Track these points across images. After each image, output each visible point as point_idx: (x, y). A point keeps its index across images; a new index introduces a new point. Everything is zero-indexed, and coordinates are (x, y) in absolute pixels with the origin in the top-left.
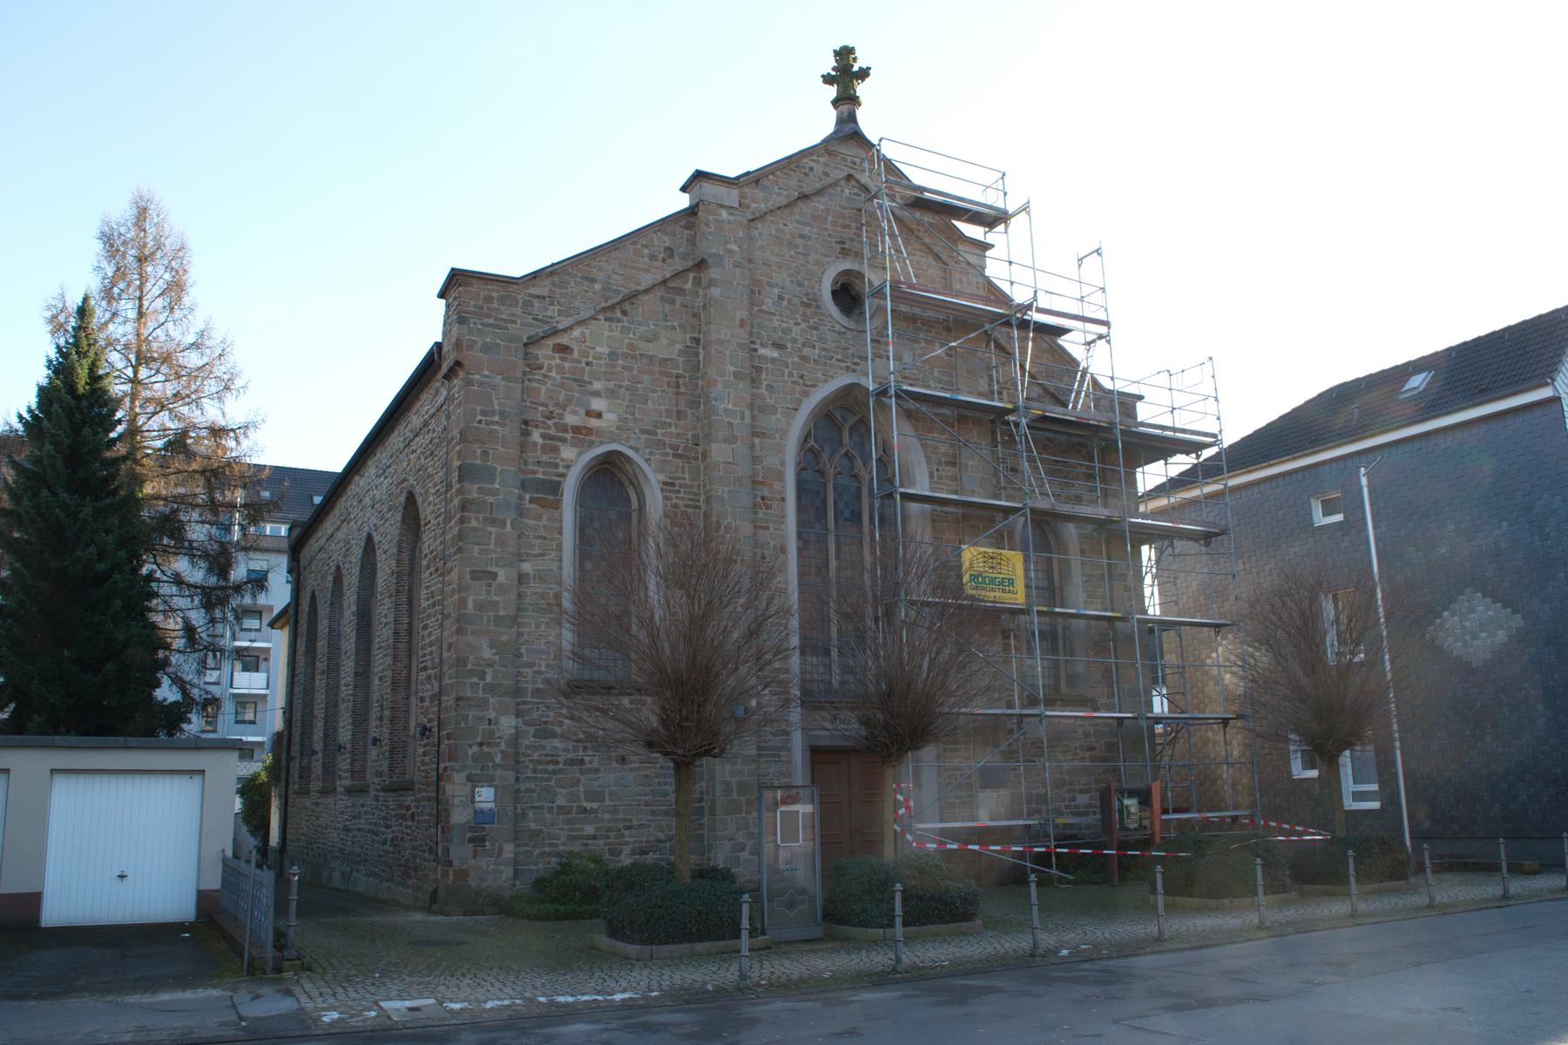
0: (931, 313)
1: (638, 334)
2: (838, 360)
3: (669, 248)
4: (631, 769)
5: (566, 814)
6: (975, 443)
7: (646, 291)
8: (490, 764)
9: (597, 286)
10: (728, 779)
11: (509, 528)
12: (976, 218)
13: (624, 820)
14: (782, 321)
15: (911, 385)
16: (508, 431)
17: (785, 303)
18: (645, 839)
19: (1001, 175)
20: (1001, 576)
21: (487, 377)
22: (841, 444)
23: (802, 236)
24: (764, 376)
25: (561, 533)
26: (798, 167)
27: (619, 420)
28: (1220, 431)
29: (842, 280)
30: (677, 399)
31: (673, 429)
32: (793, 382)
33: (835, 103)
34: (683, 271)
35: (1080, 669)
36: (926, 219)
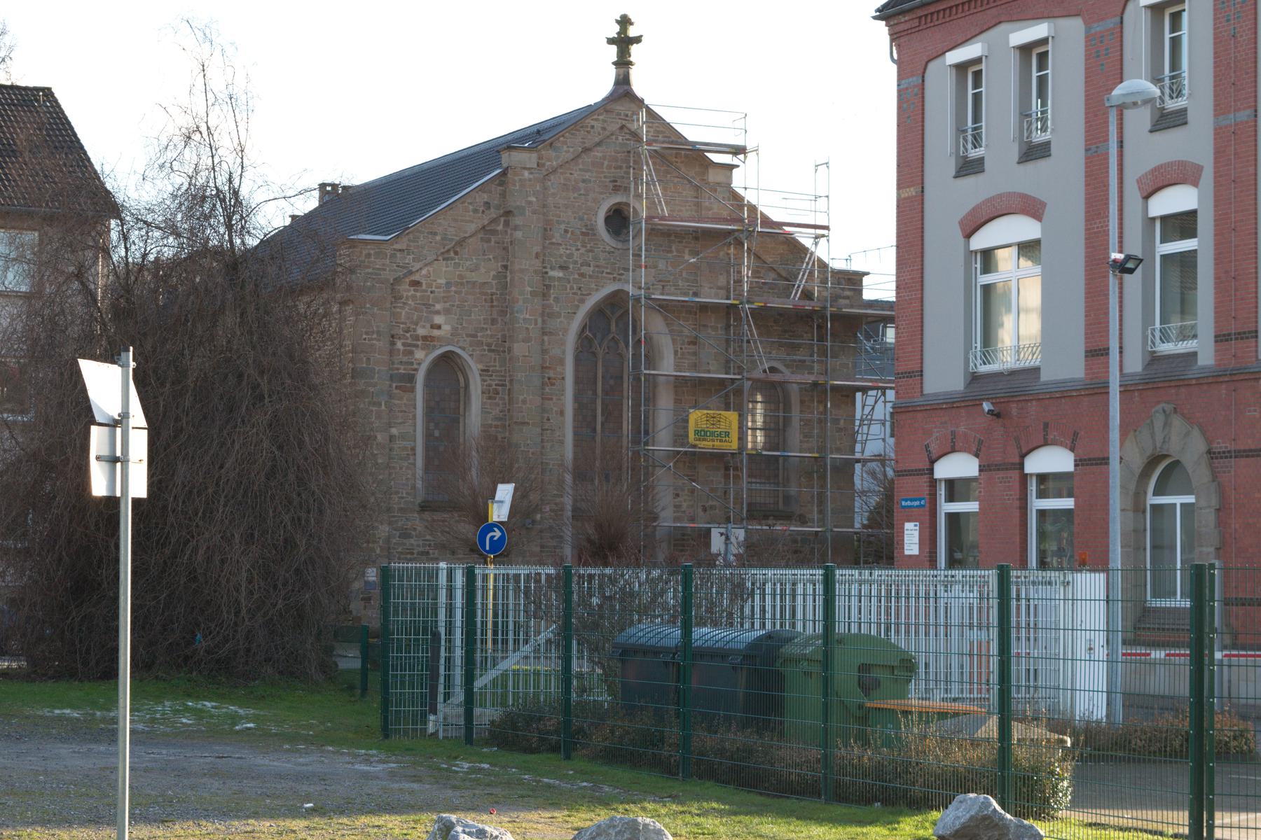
2: (607, 273)
7: (470, 236)
9: (438, 238)
11: (383, 407)
14: (567, 249)
16: (382, 344)
17: (569, 235)
20: (720, 430)
22: (609, 330)
23: (584, 181)
24: (552, 291)
25: (415, 408)
26: (582, 127)
30: (491, 311)
31: (489, 332)
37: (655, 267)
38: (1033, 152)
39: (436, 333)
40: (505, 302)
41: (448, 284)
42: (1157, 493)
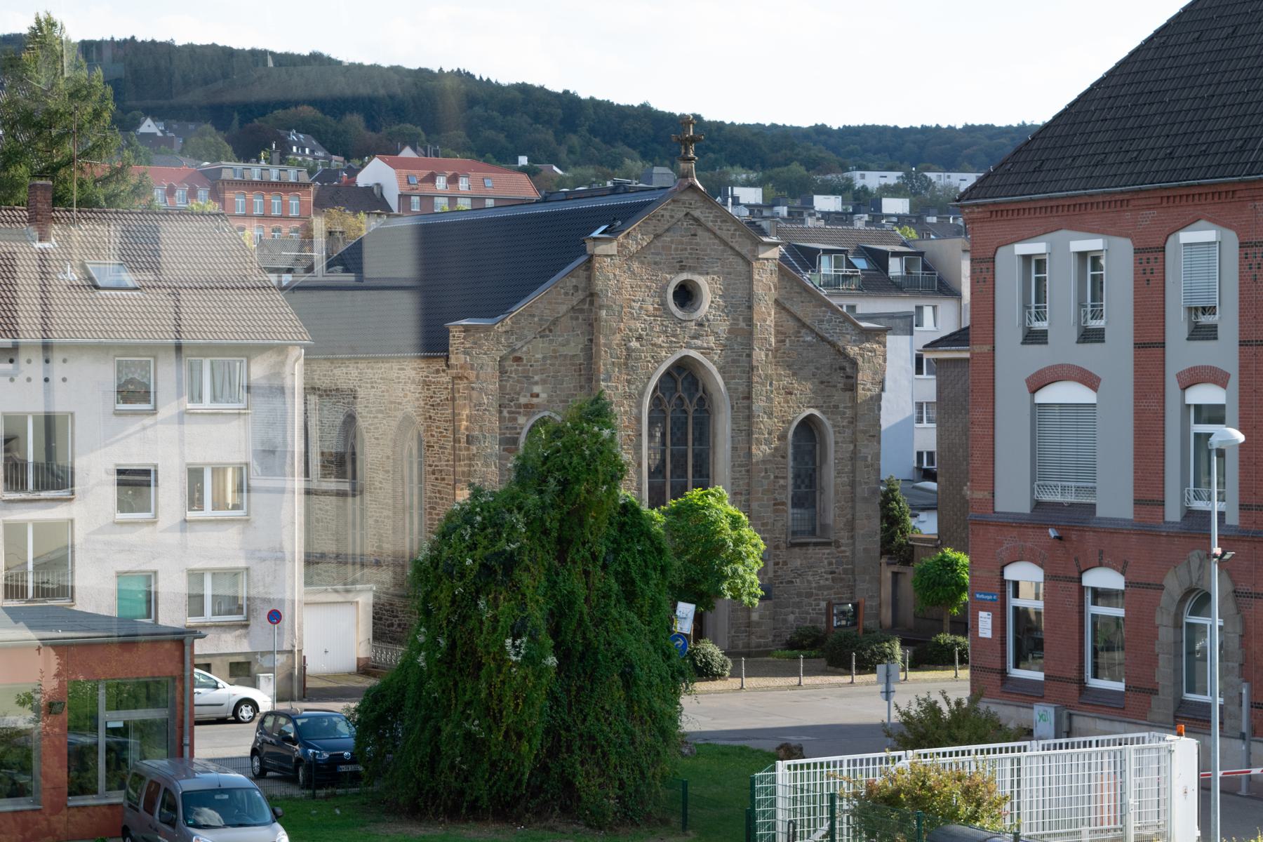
9: (536, 319)
22: (676, 391)
38: (1090, 336)
39: (535, 400)
41: (544, 358)
42: (1194, 612)
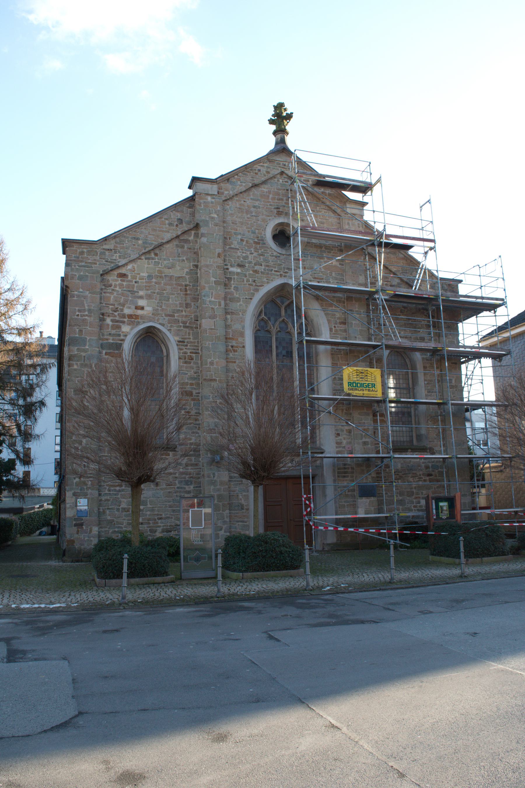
0: (330, 242)
1: (163, 265)
2: (277, 271)
3: (180, 219)
4: (161, 489)
5: (126, 512)
6: (356, 311)
7: (168, 242)
8: (85, 487)
9: (140, 242)
10: (212, 493)
12: (355, 189)
13: (158, 515)
14: (243, 253)
15: (319, 282)
16: (93, 319)
17: (244, 243)
18: (169, 524)
19: (368, 164)
21: (81, 292)
22: (280, 316)
23: (254, 207)
24: (232, 282)
26: (251, 170)
27: (154, 310)
28: (506, 297)
29: (279, 228)
30: (186, 298)
32: (249, 285)
33: (275, 133)
34: (189, 230)
35: (423, 432)
36: (327, 192)
37: (311, 268)
39: (140, 312)
40: (197, 291)
41: (150, 277)
